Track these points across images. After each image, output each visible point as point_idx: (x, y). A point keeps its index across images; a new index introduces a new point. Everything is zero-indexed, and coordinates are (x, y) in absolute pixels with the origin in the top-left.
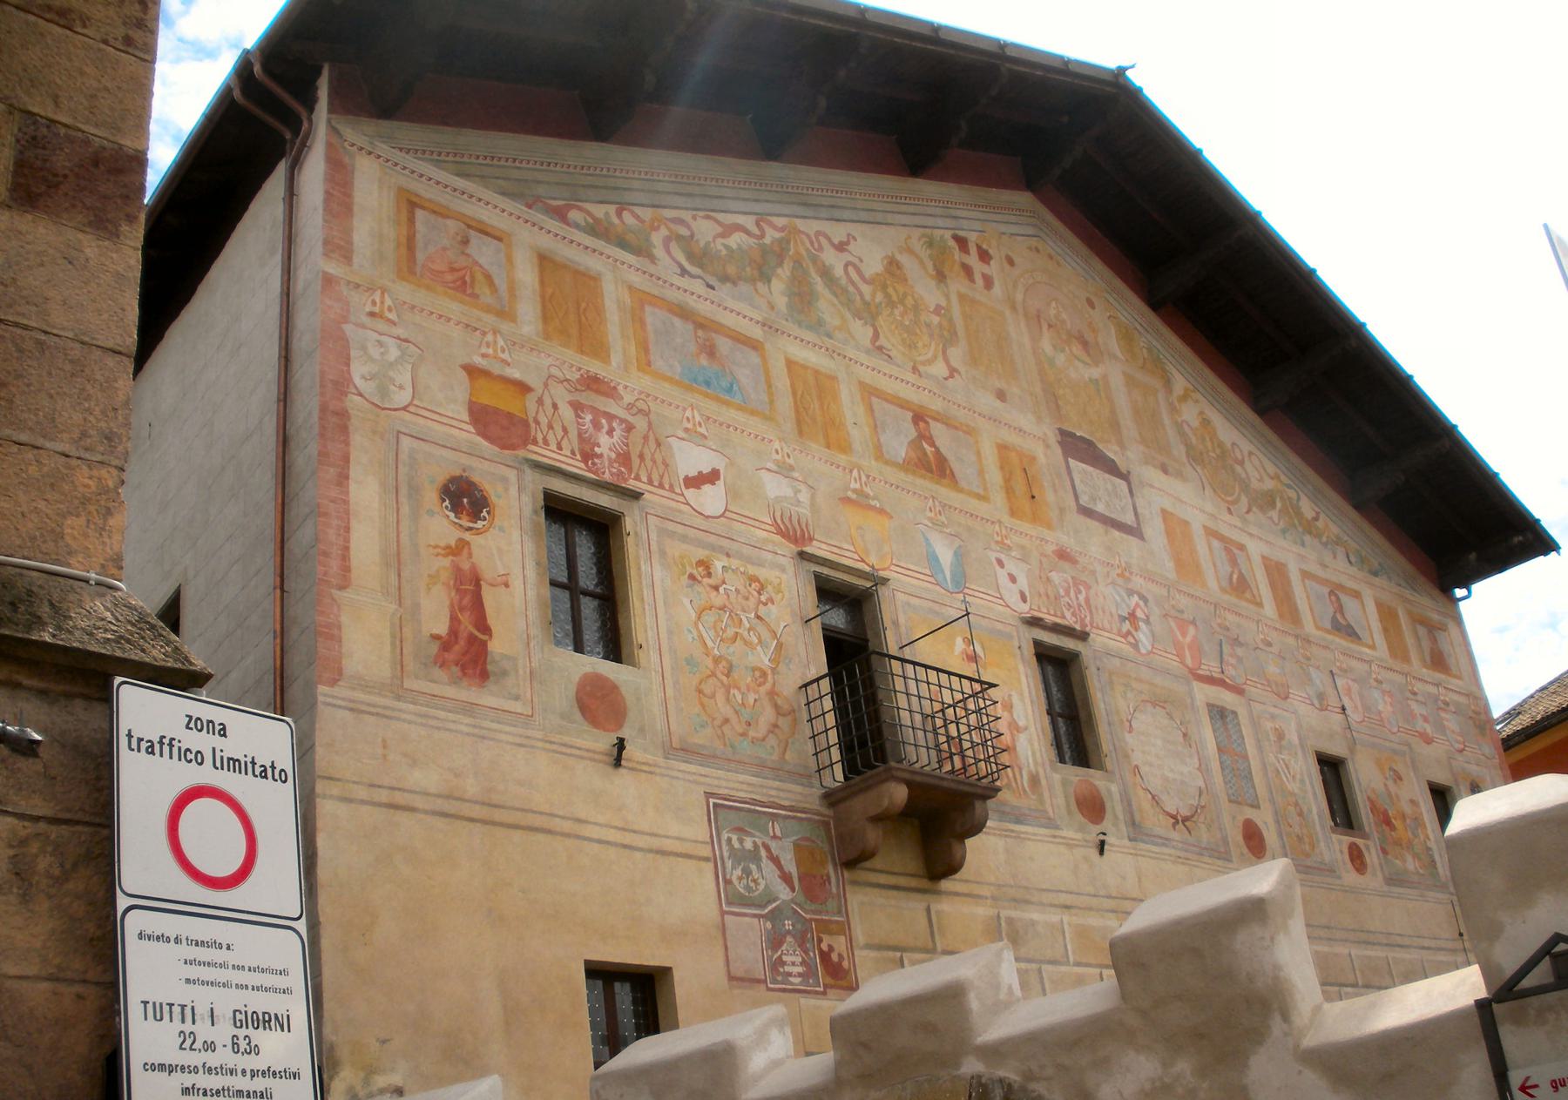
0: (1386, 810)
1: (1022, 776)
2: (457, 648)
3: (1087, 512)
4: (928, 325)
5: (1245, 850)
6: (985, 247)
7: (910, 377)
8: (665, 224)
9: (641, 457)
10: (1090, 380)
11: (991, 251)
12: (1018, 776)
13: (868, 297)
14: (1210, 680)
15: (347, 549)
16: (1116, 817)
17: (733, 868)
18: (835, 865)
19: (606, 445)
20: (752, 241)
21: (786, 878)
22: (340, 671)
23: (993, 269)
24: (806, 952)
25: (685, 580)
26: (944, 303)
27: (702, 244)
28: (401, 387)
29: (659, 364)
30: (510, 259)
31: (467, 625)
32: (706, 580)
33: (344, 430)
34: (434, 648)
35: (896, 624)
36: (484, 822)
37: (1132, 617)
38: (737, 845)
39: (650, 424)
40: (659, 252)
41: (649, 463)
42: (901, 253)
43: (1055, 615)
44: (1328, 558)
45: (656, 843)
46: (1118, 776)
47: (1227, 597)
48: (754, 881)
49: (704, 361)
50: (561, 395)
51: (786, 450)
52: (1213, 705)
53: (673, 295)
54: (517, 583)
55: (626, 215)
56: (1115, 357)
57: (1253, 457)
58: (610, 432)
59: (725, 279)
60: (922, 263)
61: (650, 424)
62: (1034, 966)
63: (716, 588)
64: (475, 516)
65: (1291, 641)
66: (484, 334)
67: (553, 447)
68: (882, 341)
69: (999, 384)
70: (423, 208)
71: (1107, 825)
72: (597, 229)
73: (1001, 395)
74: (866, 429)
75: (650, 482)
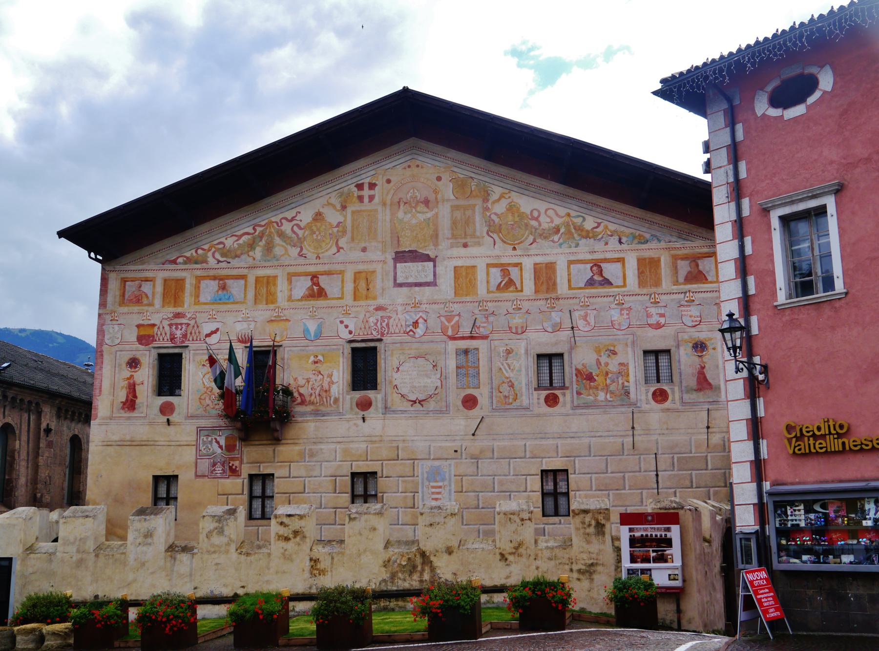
0: (591, 373)
1: (330, 400)
2: (128, 404)
3: (401, 285)
4: (330, 234)
5: (461, 407)
6: (374, 182)
8: (215, 248)
9: (191, 333)
11: (377, 182)
12: (328, 400)
13: (301, 236)
14: (463, 338)
15: (101, 386)
16: (377, 406)
17: (203, 446)
19: (179, 334)
20: (249, 237)
21: (221, 447)
22: (97, 416)
24: (224, 467)
25: (201, 366)
26: (341, 219)
27: (228, 248)
29: (202, 299)
30: (154, 286)
31: (131, 397)
33: (102, 355)
34: (121, 405)
35: (283, 359)
37: (416, 324)
38: (205, 439)
41: (193, 334)
42: (323, 207)
43: (368, 335)
44: (599, 246)
45: (178, 443)
46: (383, 390)
47: (491, 295)
48: (210, 449)
49: (220, 292)
50: (166, 323)
51: (247, 311)
52: (460, 349)
53: (212, 273)
54: (146, 383)
55: (200, 252)
56: (448, 200)
57: (550, 212)
58: (181, 330)
59: (237, 256)
60: (334, 206)
61: (196, 322)
62: (319, 463)
64: (136, 367)
65: (543, 302)
66: (143, 313)
67: (161, 340)
68: (304, 251)
69: (363, 245)
70: (128, 281)
71: (372, 409)
72: (188, 260)
73: (364, 250)
74: (286, 291)
75: (193, 340)
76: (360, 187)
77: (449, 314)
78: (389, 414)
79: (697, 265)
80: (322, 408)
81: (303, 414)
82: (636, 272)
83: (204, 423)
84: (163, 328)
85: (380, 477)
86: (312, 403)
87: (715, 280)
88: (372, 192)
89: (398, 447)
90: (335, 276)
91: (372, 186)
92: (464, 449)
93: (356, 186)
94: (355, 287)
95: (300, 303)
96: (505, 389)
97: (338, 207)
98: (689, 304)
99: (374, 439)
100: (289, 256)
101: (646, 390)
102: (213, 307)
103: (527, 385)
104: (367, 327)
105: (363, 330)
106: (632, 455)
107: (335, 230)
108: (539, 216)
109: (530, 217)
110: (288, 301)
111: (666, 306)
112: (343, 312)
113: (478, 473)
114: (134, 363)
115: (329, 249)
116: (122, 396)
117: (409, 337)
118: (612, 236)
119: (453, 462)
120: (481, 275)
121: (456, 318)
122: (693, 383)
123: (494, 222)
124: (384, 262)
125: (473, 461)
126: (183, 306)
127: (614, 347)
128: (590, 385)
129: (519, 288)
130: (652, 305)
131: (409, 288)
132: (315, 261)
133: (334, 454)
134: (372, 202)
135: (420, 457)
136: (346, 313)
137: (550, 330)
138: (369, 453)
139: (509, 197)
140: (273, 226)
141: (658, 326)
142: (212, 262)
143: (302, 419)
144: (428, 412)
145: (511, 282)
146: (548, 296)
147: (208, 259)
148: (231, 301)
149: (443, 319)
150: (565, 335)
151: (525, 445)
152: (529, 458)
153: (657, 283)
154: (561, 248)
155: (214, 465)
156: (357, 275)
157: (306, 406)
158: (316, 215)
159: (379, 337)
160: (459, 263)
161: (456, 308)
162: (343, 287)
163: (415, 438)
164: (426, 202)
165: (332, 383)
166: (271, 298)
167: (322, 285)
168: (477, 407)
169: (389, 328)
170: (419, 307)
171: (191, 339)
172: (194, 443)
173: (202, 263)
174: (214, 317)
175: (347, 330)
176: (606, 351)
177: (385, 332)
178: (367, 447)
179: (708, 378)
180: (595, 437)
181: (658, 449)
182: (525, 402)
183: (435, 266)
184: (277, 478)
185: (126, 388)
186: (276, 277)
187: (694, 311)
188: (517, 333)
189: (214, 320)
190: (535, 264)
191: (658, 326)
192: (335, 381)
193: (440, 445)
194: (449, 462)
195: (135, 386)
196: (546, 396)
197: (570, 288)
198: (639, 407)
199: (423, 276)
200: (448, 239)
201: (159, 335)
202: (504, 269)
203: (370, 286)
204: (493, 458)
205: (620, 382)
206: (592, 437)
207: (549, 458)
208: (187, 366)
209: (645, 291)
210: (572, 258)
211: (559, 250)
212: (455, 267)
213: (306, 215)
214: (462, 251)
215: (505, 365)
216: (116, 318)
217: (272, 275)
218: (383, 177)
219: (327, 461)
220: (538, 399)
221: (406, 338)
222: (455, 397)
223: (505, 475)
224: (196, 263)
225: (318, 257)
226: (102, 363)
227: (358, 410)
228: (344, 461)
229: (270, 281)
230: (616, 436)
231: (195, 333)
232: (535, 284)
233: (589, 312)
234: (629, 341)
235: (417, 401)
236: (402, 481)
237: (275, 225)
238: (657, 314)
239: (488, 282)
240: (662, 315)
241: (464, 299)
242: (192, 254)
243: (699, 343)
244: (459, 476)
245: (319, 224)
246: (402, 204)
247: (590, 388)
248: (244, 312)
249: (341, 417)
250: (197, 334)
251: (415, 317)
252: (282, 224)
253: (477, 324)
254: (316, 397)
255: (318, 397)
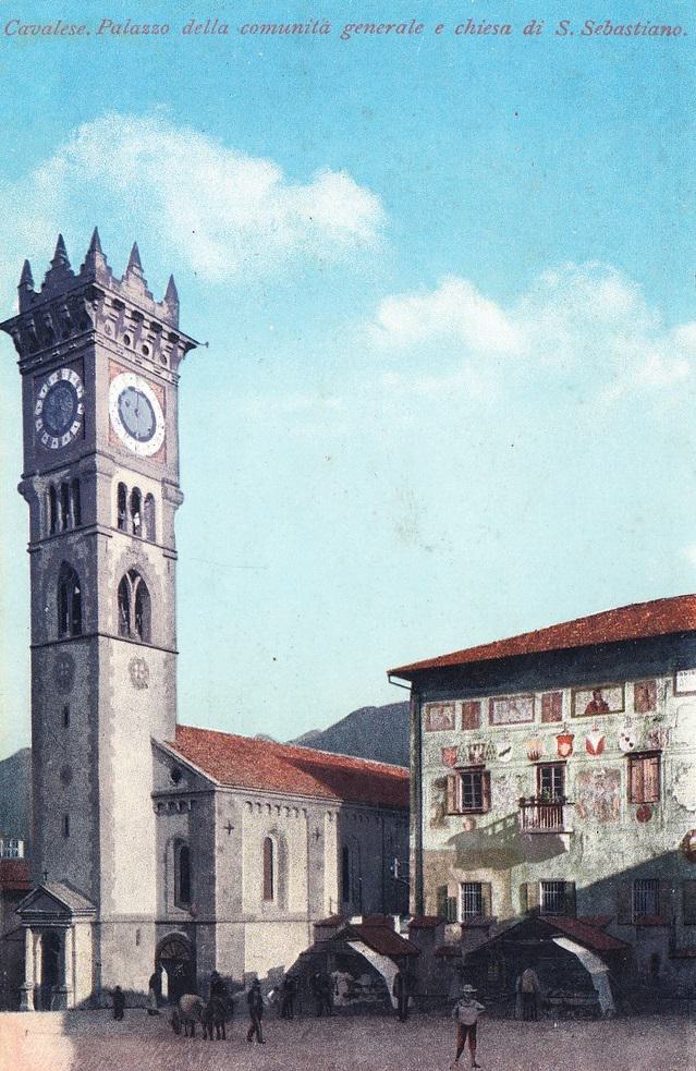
19: (477, 754)
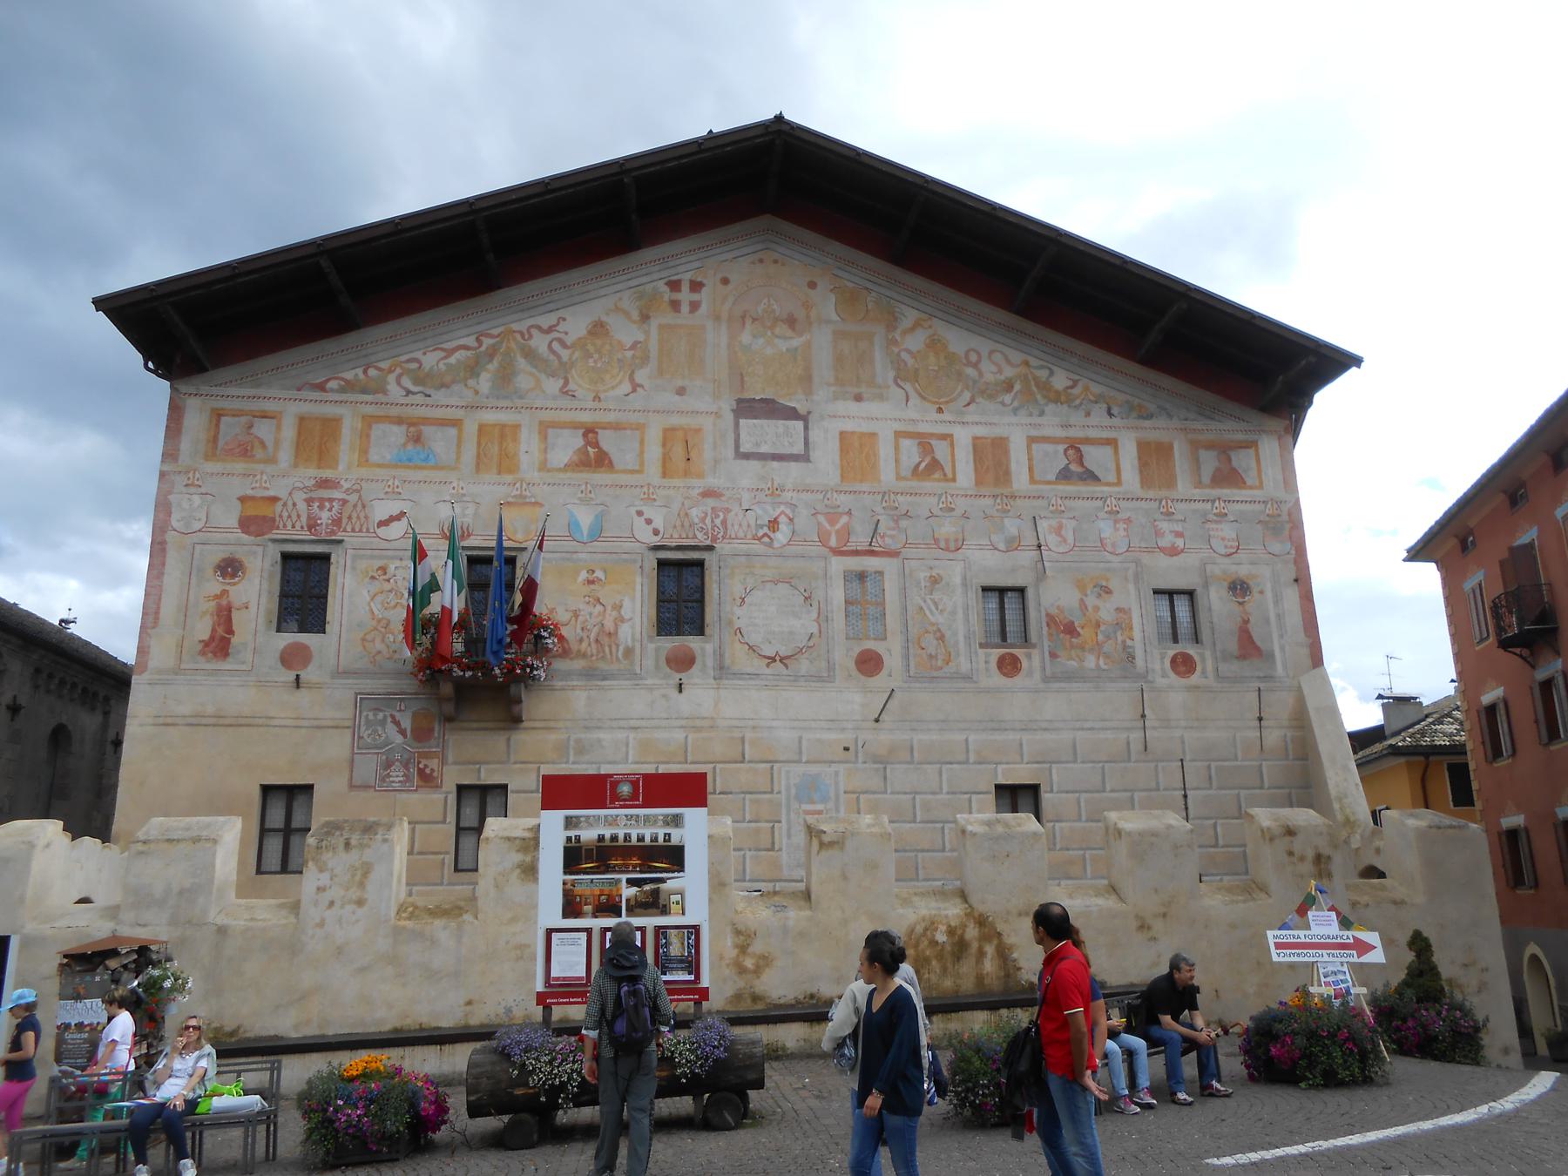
0: (1073, 623)
1: (618, 651)
2: (214, 644)
3: (747, 456)
5: (855, 672)
6: (699, 280)
7: (590, 404)
8: (401, 367)
9: (350, 518)
10: (787, 350)
11: (705, 281)
12: (614, 650)
13: (565, 358)
14: (856, 553)
15: (158, 608)
16: (704, 665)
17: (367, 729)
18: (440, 721)
19: (325, 517)
20: (469, 353)
21: (403, 732)
23: (704, 296)
25: (367, 580)
26: (641, 337)
28: (200, 520)
29: (374, 456)
30: (279, 427)
31: (220, 631)
32: (384, 577)
33: (164, 550)
34: (200, 647)
36: (214, 725)
38: (371, 717)
39: (360, 496)
40: (392, 387)
41: (354, 520)
42: (607, 314)
43: (687, 538)
44: (1077, 418)
46: (716, 637)
47: (903, 484)
49: (410, 447)
50: (299, 498)
51: (462, 484)
52: (852, 572)
53: (394, 411)
56: (828, 322)
59: (443, 385)
60: (627, 314)
61: (360, 497)
62: (594, 766)
63: (388, 581)
64: (234, 575)
65: (989, 501)
66: (255, 476)
68: (571, 386)
69: (680, 383)
70: (223, 415)
71: (695, 669)
72: (349, 387)
73: (681, 391)
75: (353, 530)
76: (675, 286)
77: (831, 511)
78: (727, 679)
79: (1230, 460)
80: (602, 665)
81: (568, 675)
82: (1136, 462)
83: (369, 685)
84: (294, 504)
85: (711, 793)
86: (584, 656)
87: (1257, 484)
88: (695, 297)
89: (743, 740)
90: (629, 432)
91: (696, 286)
92: (860, 745)
93: (666, 284)
94: (664, 455)
95: (562, 475)
96: (930, 642)
97: (635, 315)
98: (1219, 519)
99: (698, 723)
100: (543, 392)
101: (1161, 654)
102: (393, 472)
103: (967, 638)
104: (687, 524)
105: (679, 528)
106: (1145, 761)
107: (629, 354)
108: (979, 361)
109: (964, 361)
110: (540, 470)
111: (1184, 521)
112: (642, 496)
113: (886, 788)
114: (230, 568)
115: (617, 385)
116: (203, 629)
117: (762, 546)
118: (1096, 402)
119: (841, 768)
120: (885, 450)
121: (844, 519)
122: (1232, 645)
123: (906, 364)
124: (717, 415)
125: (876, 766)
126: (334, 466)
127: (1107, 580)
128: (1070, 641)
129: (950, 475)
130: (1163, 517)
131: (762, 463)
132: (590, 404)
133: (624, 749)
134: (697, 313)
135: (781, 759)
136: (649, 498)
137: (1002, 546)
138: (689, 749)
139: (930, 327)
140: (514, 339)
141: (1173, 552)
142: (395, 392)
143: (564, 683)
144: (796, 678)
145: (935, 465)
146: (998, 491)
147: (389, 387)
148: (432, 463)
149: (821, 518)
150: (1027, 557)
151: (967, 740)
152: (975, 763)
153: (1171, 483)
154: (1015, 414)
155: (388, 765)
156: (668, 434)
157: (571, 659)
158: (595, 326)
159: (708, 542)
160: (849, 426)
161: (843, 501)
162: (642, 453)
163: (775, 724)
164: (791, 322)
165: (620, 620)
166: (507, 464)
167: (605, 445)
168: (883, 671)
169: (726, 529)
170: (779, 495)
171: (349, 529)
172: (349, 723)
173: (375, 392)
174: (396, 490)
175: (650, 528)
176: (1095, 587)
177: (720, 536)
178: (686, 737)
179: (1255, 639)
180: (1083, 729)
181: (1184, 752)
182: (965, 666)
183: (806, 428)
184: (512, 792)
185: (212, 615)
186: (517, 427)
187: (1227, 531)
188: (947, 549)
189: (399, 497)
190: (975, 439)
191: (1173, 552)
192: (627, 617)
193: (818, 736)
194: (834, 767)
195: (230, 611)
196: (999, 658)
197: (1032, 480)
198: (1151, 682)
199: (786, 444)
200: (829, 385)
201: (285, 519)
202: (925, 443)
203: (693, 455)
204: (911, 762)
205: (1120, 638)
206: (1079, 729)
207: (1007, 763)
208: (340, 580)
209: (1151, 494)
210: (1034, 433)
211: (1014, 419)
212: (841, 433)
213: (576, 324)
214: (853, 407)
215: (929, 601)
216: (197, 483)
217: (510, 423)
218: (715, 274)
219: (610, 763)
220: (986, 662)
221: (757, 547)
222: (844, 655)
223: (933, 793)
224: (364, 391)
225: (597, 398)
226: (163, 564)
227: (668, 670)
228: (642, 763)
229: (507, 433)
230: (1118, 729)
231: (358, 518)
232: (976, 470)
233: (1064, 521)
234: (1131, 572)
235: (778, 658)
236: (751, 800)
237: (518, 337)
238: (1171, 532)
239: (897, 461)
240: (1179, 535)
241: (858, 487)
242: (357, 375)
243: (1238, 582)
244: (854, 792)
245: (598, 342)
246: (748, 322)
247: (1072, 647)
248: (455, 484)
249: (637, 682)
250: (363, 520)
251: (771, 512)
252: (531, 336)
253: (881, 530)
254: (589, 645)
255: (594, 645)
